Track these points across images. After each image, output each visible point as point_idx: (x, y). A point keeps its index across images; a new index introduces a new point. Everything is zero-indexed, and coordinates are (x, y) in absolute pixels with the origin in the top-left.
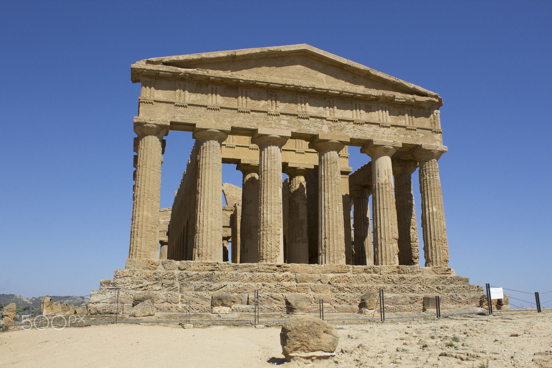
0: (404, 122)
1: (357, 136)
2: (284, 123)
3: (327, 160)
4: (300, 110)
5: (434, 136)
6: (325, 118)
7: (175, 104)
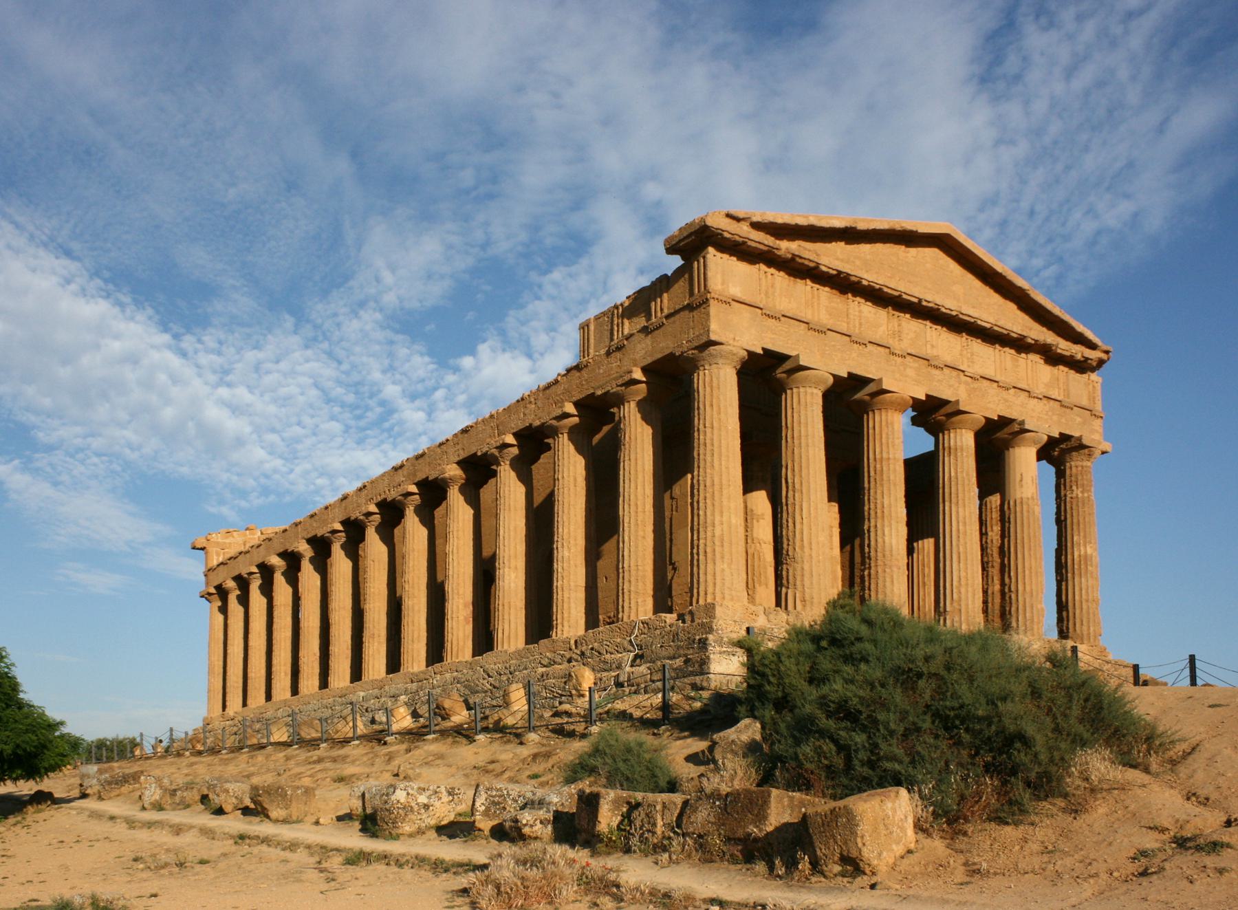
0: (1057, 393)
1: (1001, 410)
2: (910, 372)
3: (962, 450)
4: (929, 351)
5: (1094, 423)
6: (963, 371)
7: (764, 311)
